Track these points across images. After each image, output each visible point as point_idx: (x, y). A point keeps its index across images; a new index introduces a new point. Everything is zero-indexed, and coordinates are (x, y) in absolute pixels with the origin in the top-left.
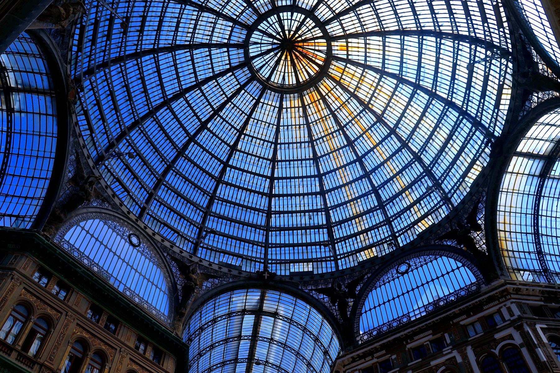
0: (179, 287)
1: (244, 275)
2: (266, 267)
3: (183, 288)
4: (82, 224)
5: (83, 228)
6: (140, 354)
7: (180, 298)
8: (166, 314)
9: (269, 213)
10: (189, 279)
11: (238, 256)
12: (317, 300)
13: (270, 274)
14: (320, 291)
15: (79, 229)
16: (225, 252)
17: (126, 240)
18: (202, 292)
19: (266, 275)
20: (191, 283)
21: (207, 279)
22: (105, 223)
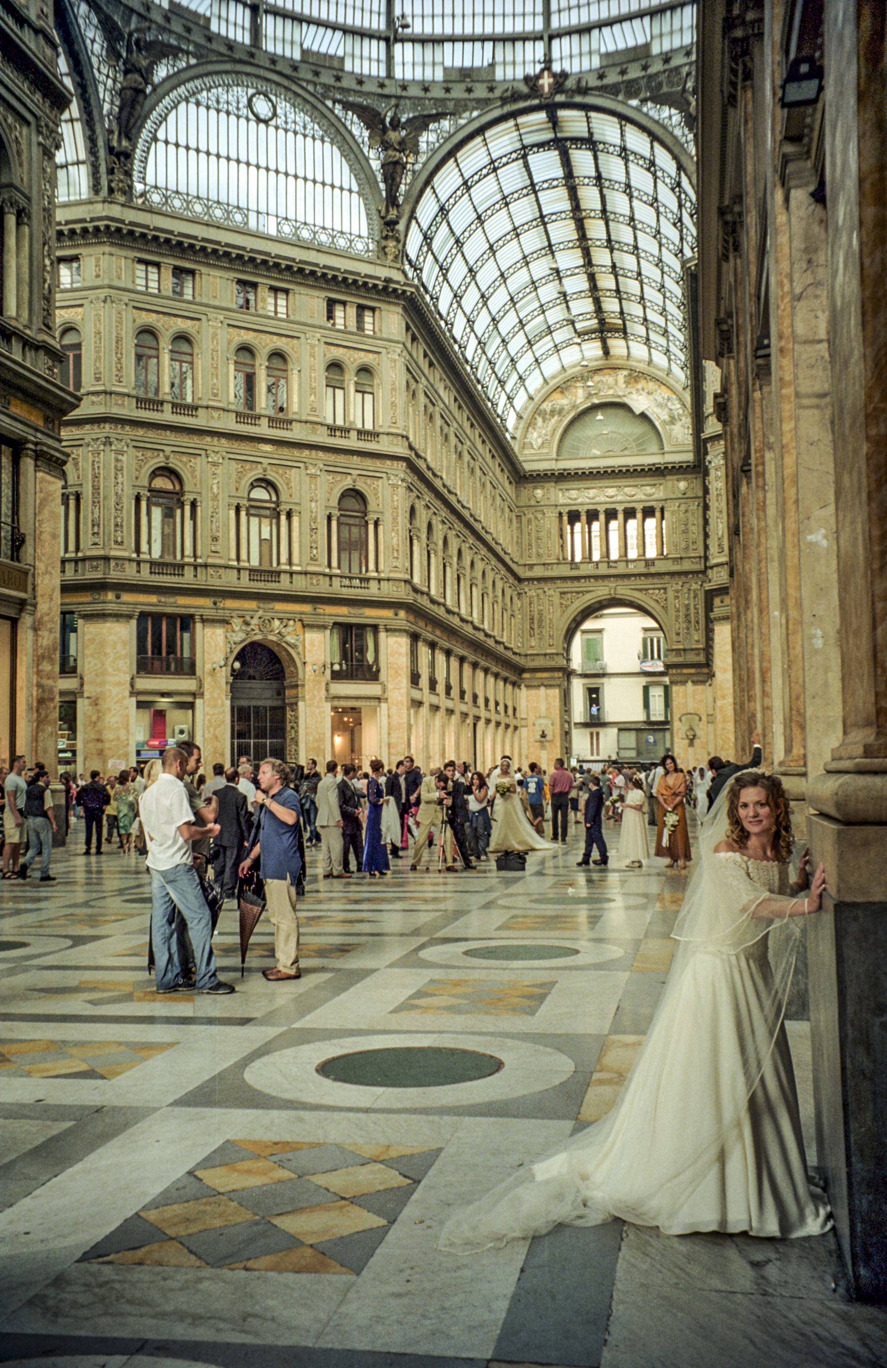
1: (498, 93)
3: (383, 166)
4: (161, 135)
5: (167, 142)
6: (339, 331)
7: (382, 186)
8: (364, 233)
10: (386, 146)
11: (483, 39)
12: (657, 122)
13: (554, 75)
15: (161, 145)
17: (248, 119)
18: (422, 159)
19: (546, 82)
21: (425, 127)
22: (198, 104)
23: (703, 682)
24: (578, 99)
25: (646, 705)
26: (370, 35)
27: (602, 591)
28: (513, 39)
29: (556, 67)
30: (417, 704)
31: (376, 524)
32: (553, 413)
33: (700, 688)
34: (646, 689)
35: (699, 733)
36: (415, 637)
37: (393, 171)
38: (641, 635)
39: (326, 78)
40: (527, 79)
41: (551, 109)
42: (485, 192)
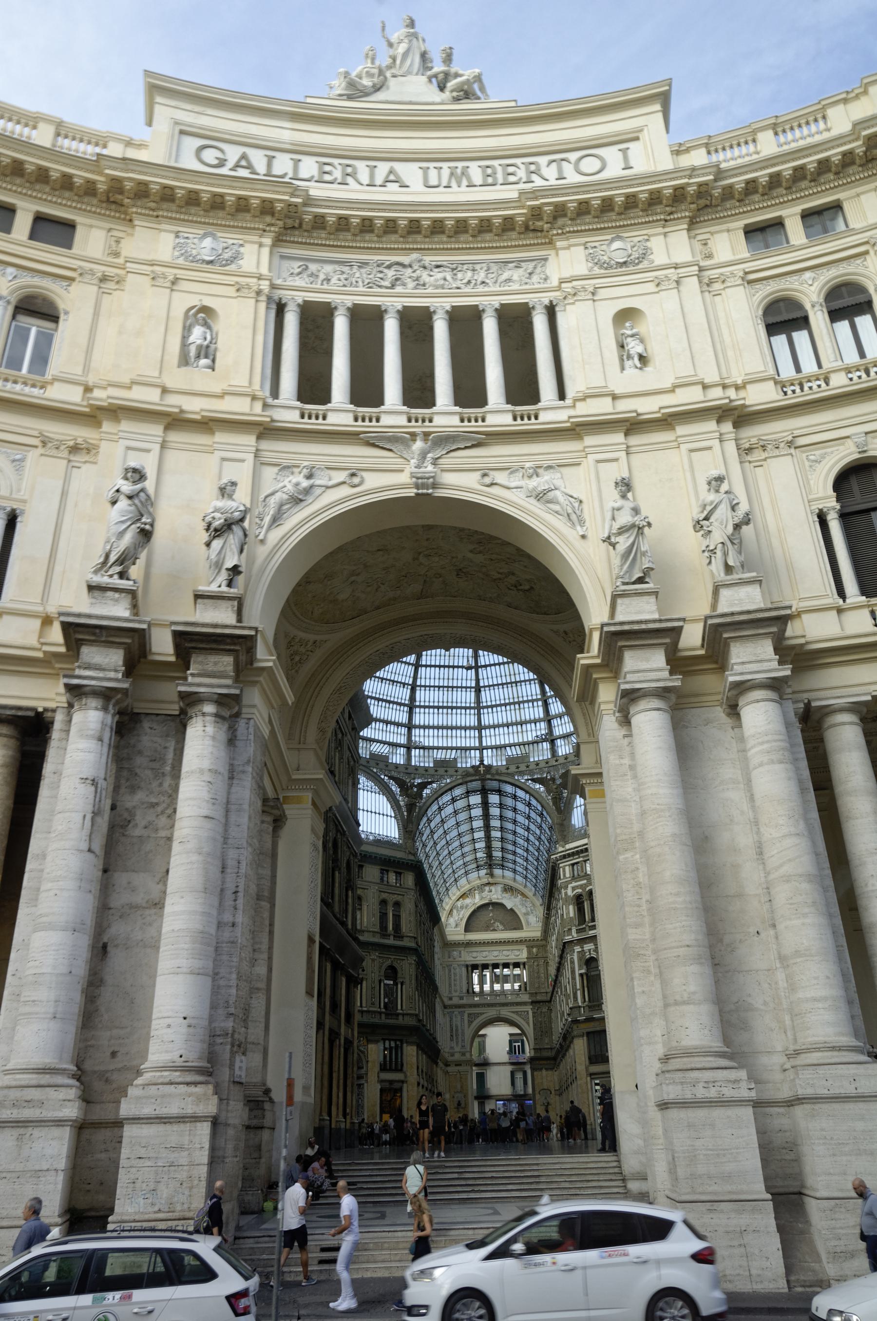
0: (402, 803)
2: (482, 761)
9: (478, 689)
14: (533, 780)
16: (438, 748)
19: (482, 769)
20: (412, 796)
23: (552, 1069)
24: (497, 777)
25: (513, 1083)
26: (400, 746)
27: (492, 1013)
28: (466, 749)
29: (486, 763)
30: (419, 1084)
31: (402, 984)
32: (462, 907)
33: (550, 1072)
34: (512, 1074)
35: (552, 1101)
36: (418, 1046)
37: (410, 807)
38: (508, 1038)
39: (382, 765)
40: (473, 767)
41: (483, 780)
42: (449, 810)
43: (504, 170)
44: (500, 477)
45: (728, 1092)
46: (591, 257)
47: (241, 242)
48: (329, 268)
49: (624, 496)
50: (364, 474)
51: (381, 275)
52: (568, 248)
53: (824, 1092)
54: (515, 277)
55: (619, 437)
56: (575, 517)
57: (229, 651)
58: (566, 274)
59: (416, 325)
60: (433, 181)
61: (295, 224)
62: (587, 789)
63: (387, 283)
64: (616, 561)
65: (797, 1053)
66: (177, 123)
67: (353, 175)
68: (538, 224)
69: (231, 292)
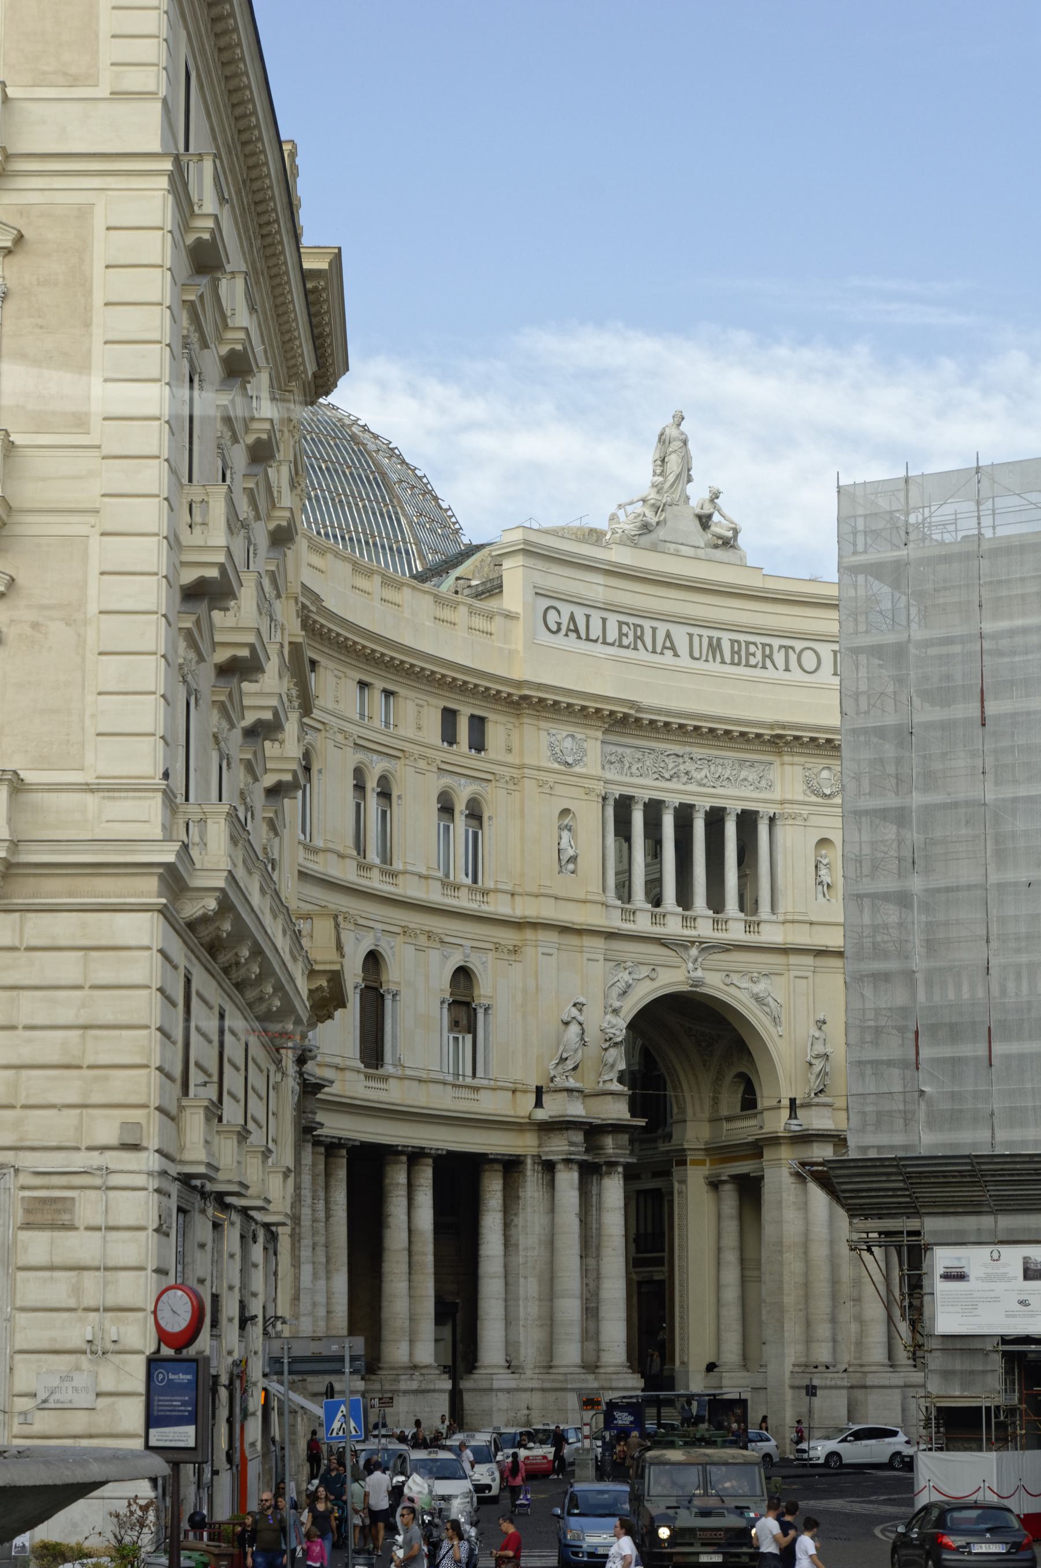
43: (747, 648)
44: (735, 978)
45: (839, 1383)
46: (807, 782)
47: (584, 736)
48: (628, 751)
49: (820, 1029)
50: (658, 968)
51: (662, 765)
52: (792, 764)
53: (876, 1384)
54: (750, 779)
55: (809, 960)
56: (776, 1021)
57: (627, 1132)
58: (789, 797)
59: (684, 816)
60: (697, 655)
61: (622, 722)
62: (688, 1158)
63: (667, 776)
64: (813, 1078)
65: (861, 1366)
66: (535, 587)
67: (641, 638)
68: (779, 742)
69: (579, 793)
